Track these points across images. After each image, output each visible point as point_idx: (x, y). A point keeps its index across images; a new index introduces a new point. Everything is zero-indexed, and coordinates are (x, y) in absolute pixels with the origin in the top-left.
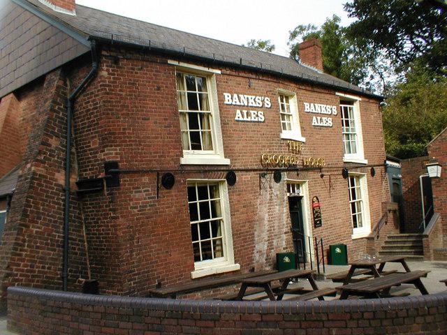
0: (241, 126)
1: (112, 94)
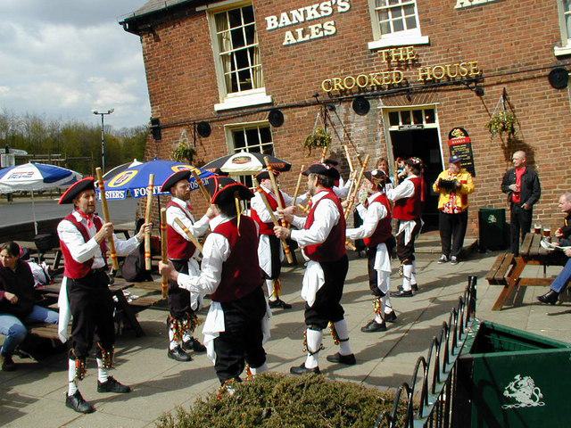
0: (291, 52)
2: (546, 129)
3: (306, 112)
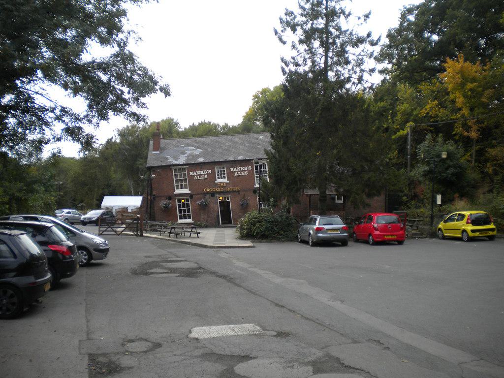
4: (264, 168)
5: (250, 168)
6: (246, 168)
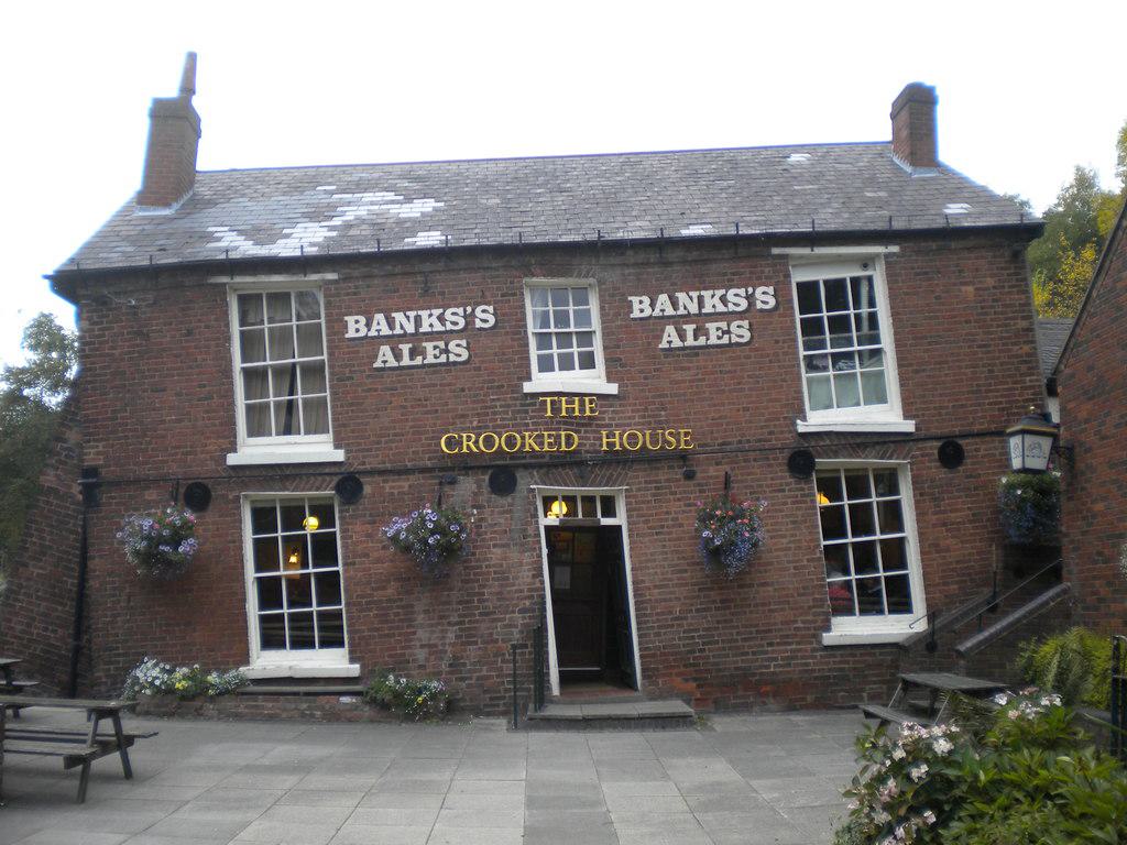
1: (95, 356)
2: (784, 536)
3: (406, 484)
4: (857, 305)
5: (765, 297)
6: (737, 298)
